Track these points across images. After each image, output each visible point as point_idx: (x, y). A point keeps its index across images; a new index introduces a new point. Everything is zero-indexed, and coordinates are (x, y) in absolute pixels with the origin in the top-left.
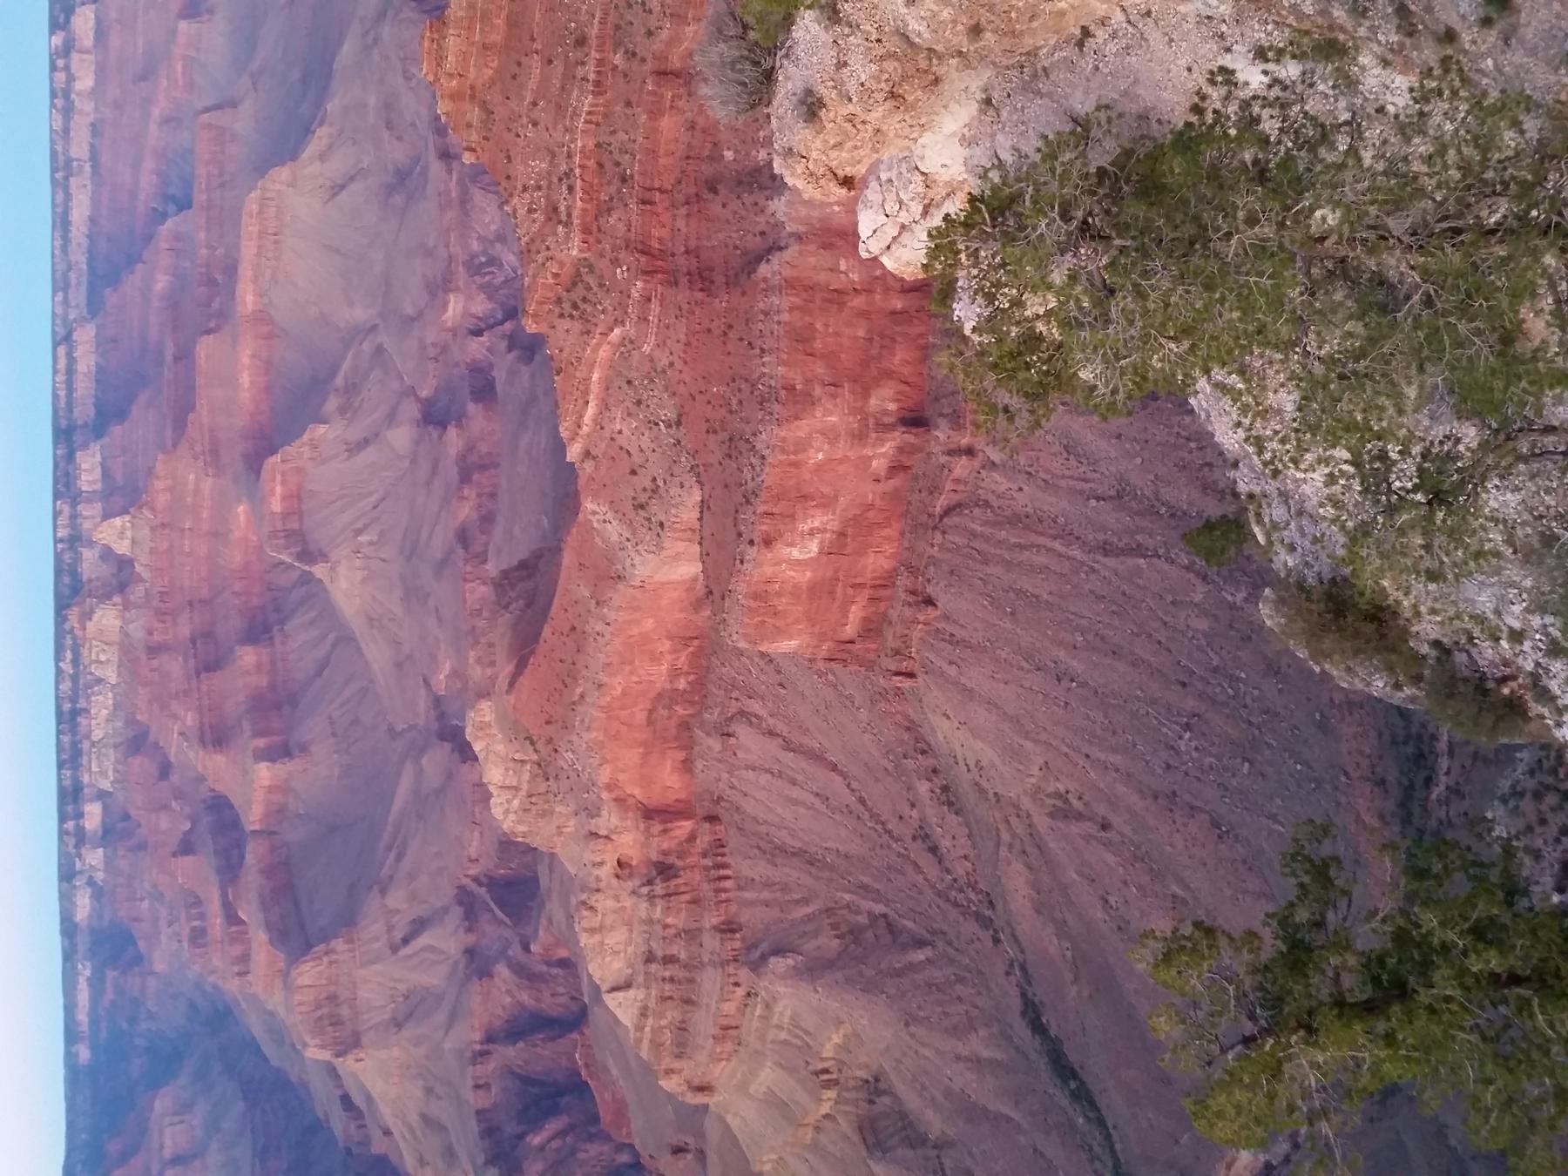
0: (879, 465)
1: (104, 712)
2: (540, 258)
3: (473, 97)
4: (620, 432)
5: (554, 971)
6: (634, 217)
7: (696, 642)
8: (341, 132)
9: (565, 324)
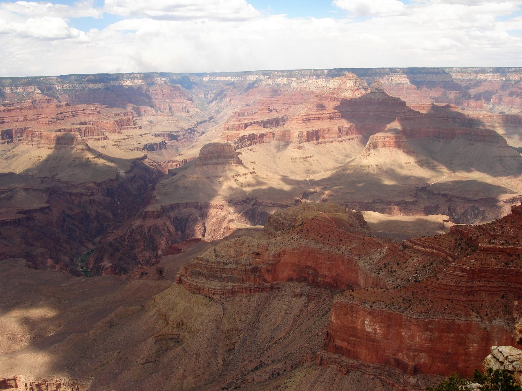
0: (400, 356)
4: (413, 260)
5: (222, 230)
7: (335, 284)
9: (453, 241)
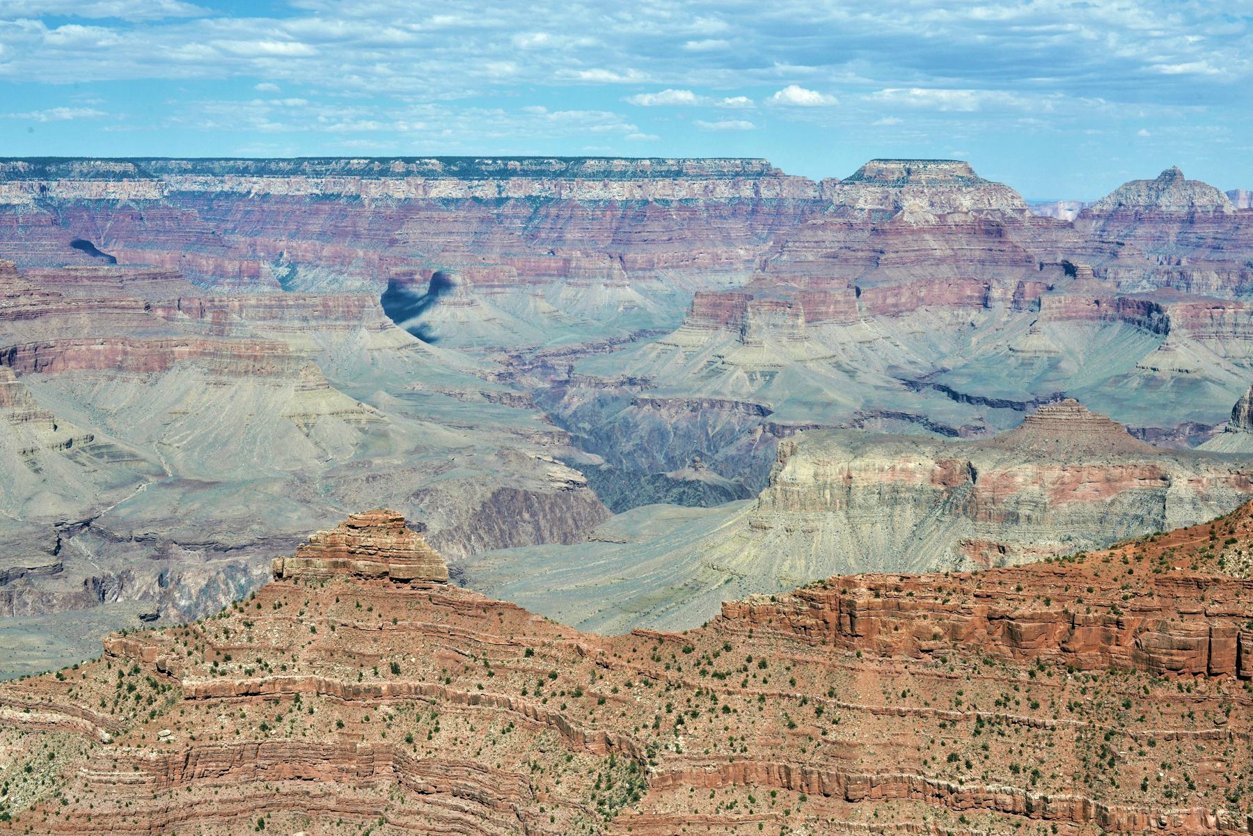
3: (335, 565)
9: (113, 679)
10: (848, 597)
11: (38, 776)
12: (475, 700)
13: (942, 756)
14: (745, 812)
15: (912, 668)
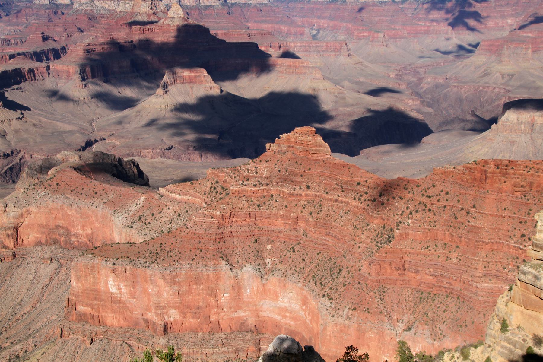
1: (107, 6)
2: (232, 175)
3: (289, 147)
4: (169, 209)
6: (244, 210)
7: (91, 244)
8: (336, 96)
9: (209, 185)
10: (484, 168)
11: (182, 218)
12: (336, 201)
13: (518, 234)
14: (433, 250)
15: (510, 198)
